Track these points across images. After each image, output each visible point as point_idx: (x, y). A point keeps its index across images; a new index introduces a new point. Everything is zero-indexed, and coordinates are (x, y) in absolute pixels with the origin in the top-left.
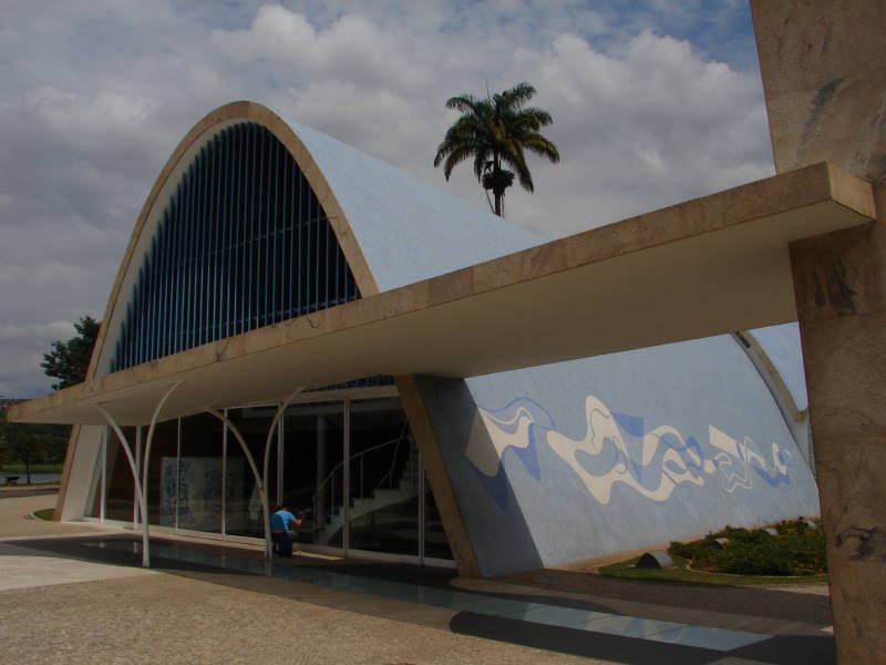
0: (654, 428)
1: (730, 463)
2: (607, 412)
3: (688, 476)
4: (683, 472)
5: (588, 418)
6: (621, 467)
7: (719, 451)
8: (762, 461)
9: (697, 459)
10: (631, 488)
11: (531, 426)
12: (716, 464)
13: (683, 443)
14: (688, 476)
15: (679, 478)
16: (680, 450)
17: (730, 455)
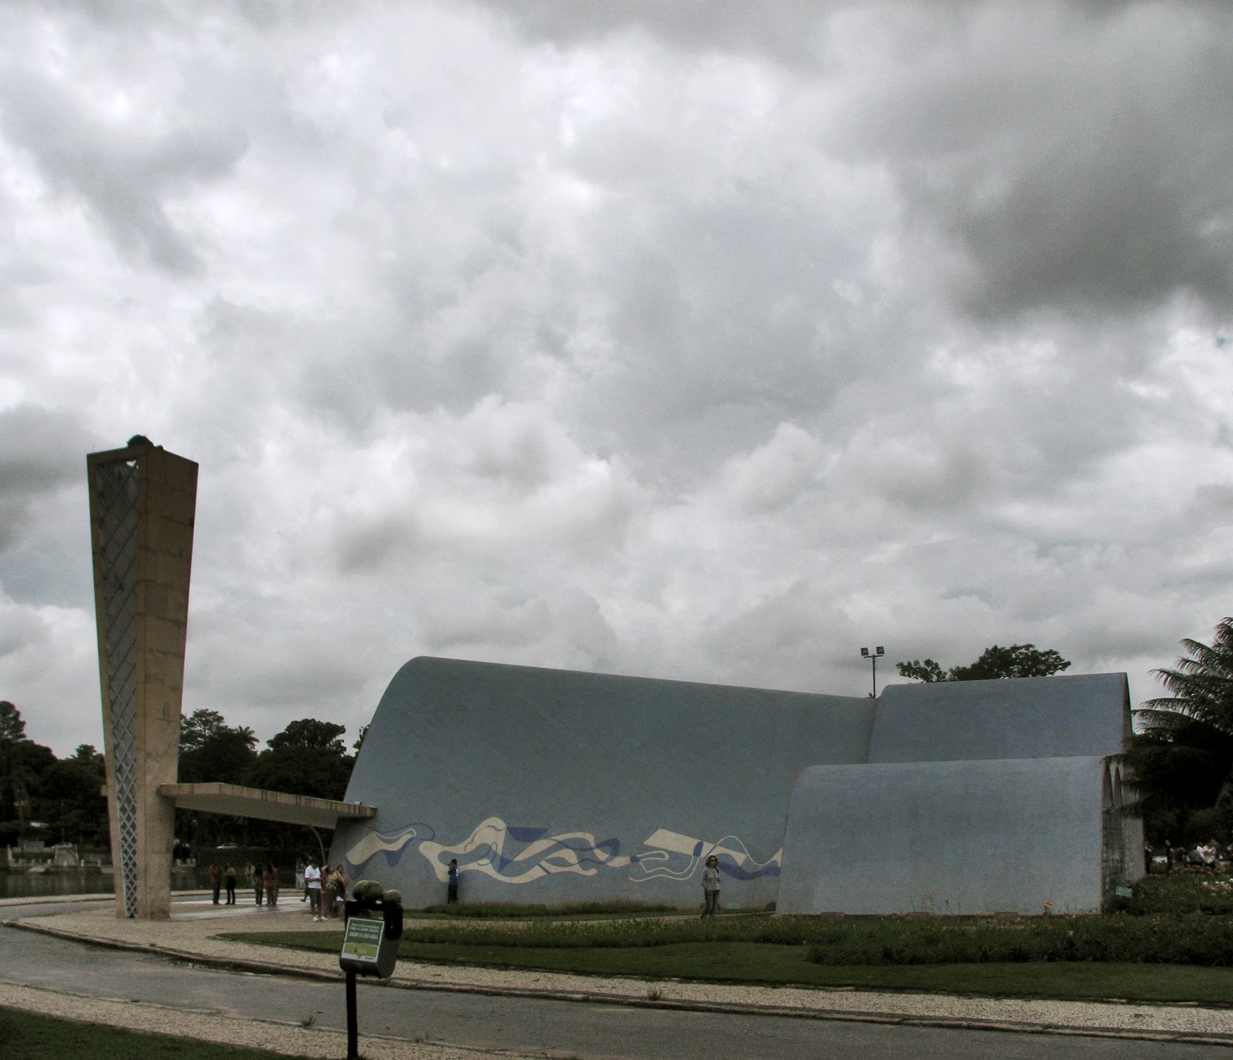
0: (558, 835)
1: (667, 857)
2: (501, 824)
3: (577, 869)
4: (572, 865)
5: (477, 829)
6: (485, 861)
7: (653, 849)
8: (740, 858)
9: (601, 855)
10: (487, 875)
11: (413, 838)
12: (634, 860)
13: (593, 844)
14: (577, 869)
15: (554, 869)
16: (581, 848)
17: (664, 850)
